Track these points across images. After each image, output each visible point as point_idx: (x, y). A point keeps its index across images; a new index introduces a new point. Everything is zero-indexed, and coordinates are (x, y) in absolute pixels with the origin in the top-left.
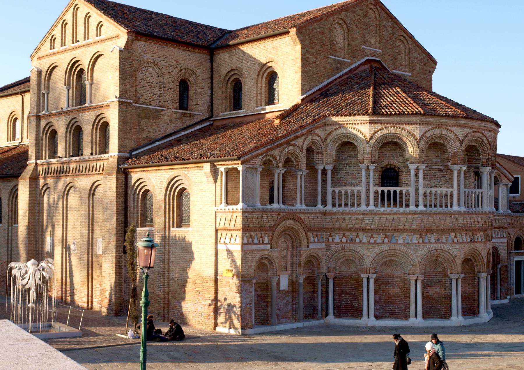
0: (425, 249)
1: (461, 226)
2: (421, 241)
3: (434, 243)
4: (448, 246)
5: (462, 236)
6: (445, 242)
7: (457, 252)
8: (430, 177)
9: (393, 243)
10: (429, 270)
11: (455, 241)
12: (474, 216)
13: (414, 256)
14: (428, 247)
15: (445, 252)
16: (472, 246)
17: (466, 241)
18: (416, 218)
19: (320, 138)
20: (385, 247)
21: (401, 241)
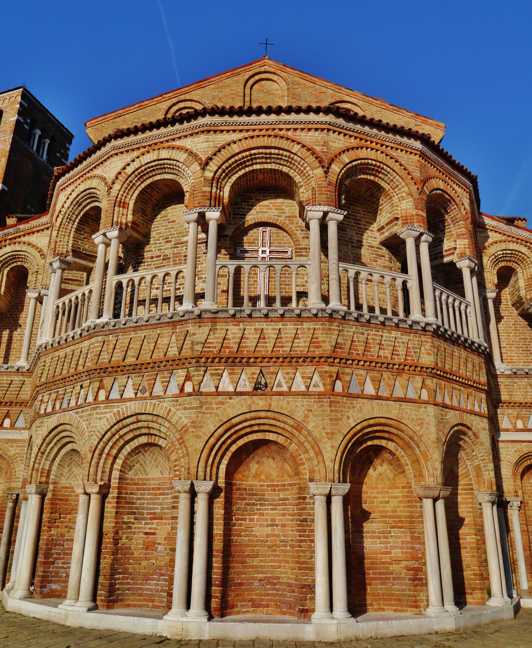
0: (108, 415)
1: (199, 348)
2: (102, 395)
3: (130, 400)
4: (165, 405)
5: (212, 375)
6: (162, 393)
7: (190, 417)
8: (174, 261)
9: (65, 410)
10: (160, 475)
11: (189, 388)
12: (264, 325)
13: (87, 434)
14: (115, 410)
15: (160, 420)
16: (260, 403)
17: (231, 389)
18: (93, 343)
19: (37, 248)
20: (53, 421)
21: (73, 404)
